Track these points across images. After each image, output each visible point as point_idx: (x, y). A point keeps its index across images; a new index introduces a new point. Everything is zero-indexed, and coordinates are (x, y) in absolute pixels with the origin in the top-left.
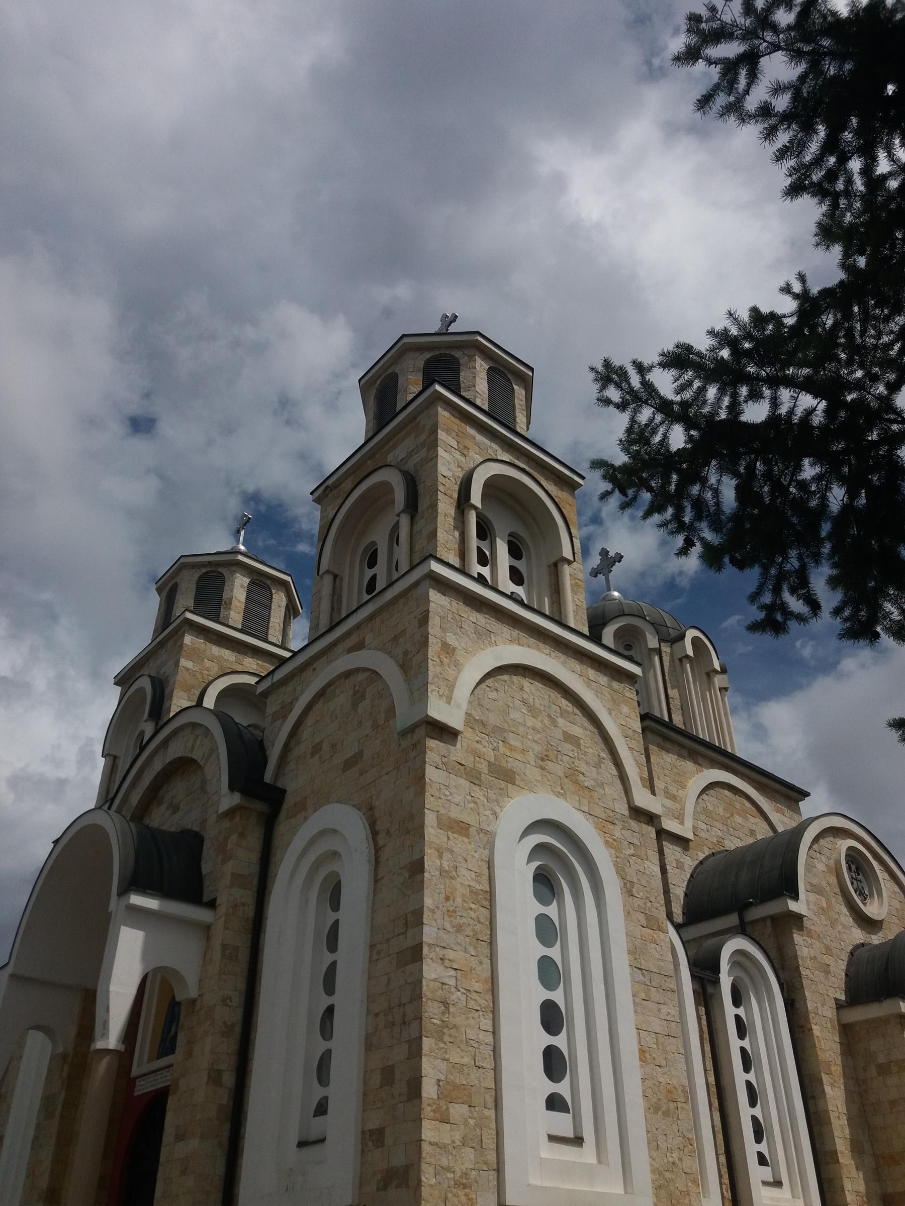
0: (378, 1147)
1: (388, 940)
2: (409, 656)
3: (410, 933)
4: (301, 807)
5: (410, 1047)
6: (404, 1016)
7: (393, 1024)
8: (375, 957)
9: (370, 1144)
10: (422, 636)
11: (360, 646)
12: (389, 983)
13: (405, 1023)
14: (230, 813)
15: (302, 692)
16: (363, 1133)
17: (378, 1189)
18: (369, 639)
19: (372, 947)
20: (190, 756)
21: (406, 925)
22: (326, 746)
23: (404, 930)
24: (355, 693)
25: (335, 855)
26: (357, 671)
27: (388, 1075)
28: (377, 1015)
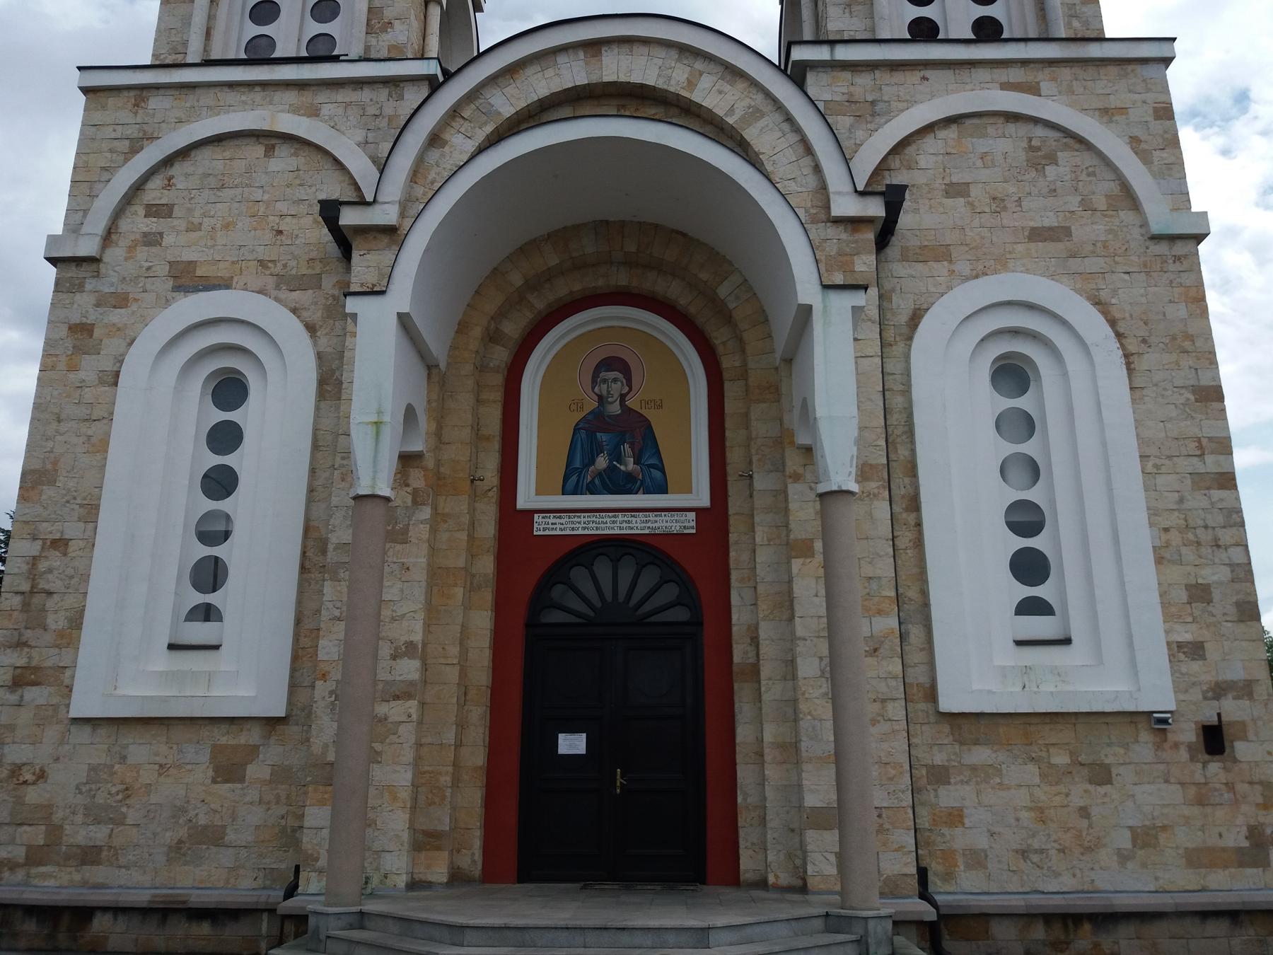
0: (1193, 659)
1: (1170, 457)
2: (1143, 146)
3: (1209, 459)
4: (942, 254)
5: (1232, 571)
6: (1216, 539)
7: (1199, 543)
8: (1150, 468)
9: (1182, 656)
10: (1165, 132)
11: (1034, 90)
12: (1181, 500)
13: (1218, 546)
14: (854, 223)
15: (911, 103)
16: (1168, 643)
17: (1205, 698)
18: (1045, 87)
19: (1143, 457)
20: (684, 93)
21: (1200, 447)
22: (975, 191)
23: (1198, 453)
24: (1031, 148)
25: (1015, 332)
26: (1036, 121)
27: (1200, 593)
28: (1166, 530)
